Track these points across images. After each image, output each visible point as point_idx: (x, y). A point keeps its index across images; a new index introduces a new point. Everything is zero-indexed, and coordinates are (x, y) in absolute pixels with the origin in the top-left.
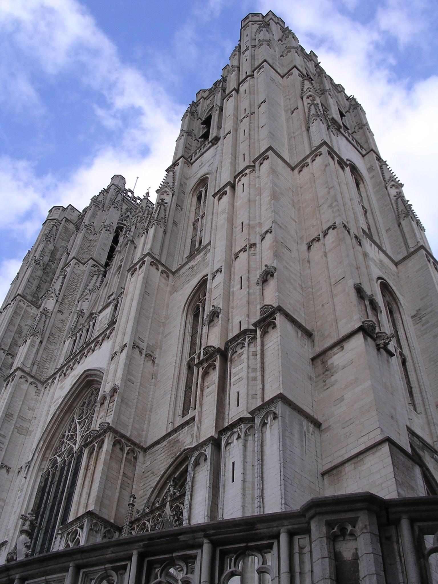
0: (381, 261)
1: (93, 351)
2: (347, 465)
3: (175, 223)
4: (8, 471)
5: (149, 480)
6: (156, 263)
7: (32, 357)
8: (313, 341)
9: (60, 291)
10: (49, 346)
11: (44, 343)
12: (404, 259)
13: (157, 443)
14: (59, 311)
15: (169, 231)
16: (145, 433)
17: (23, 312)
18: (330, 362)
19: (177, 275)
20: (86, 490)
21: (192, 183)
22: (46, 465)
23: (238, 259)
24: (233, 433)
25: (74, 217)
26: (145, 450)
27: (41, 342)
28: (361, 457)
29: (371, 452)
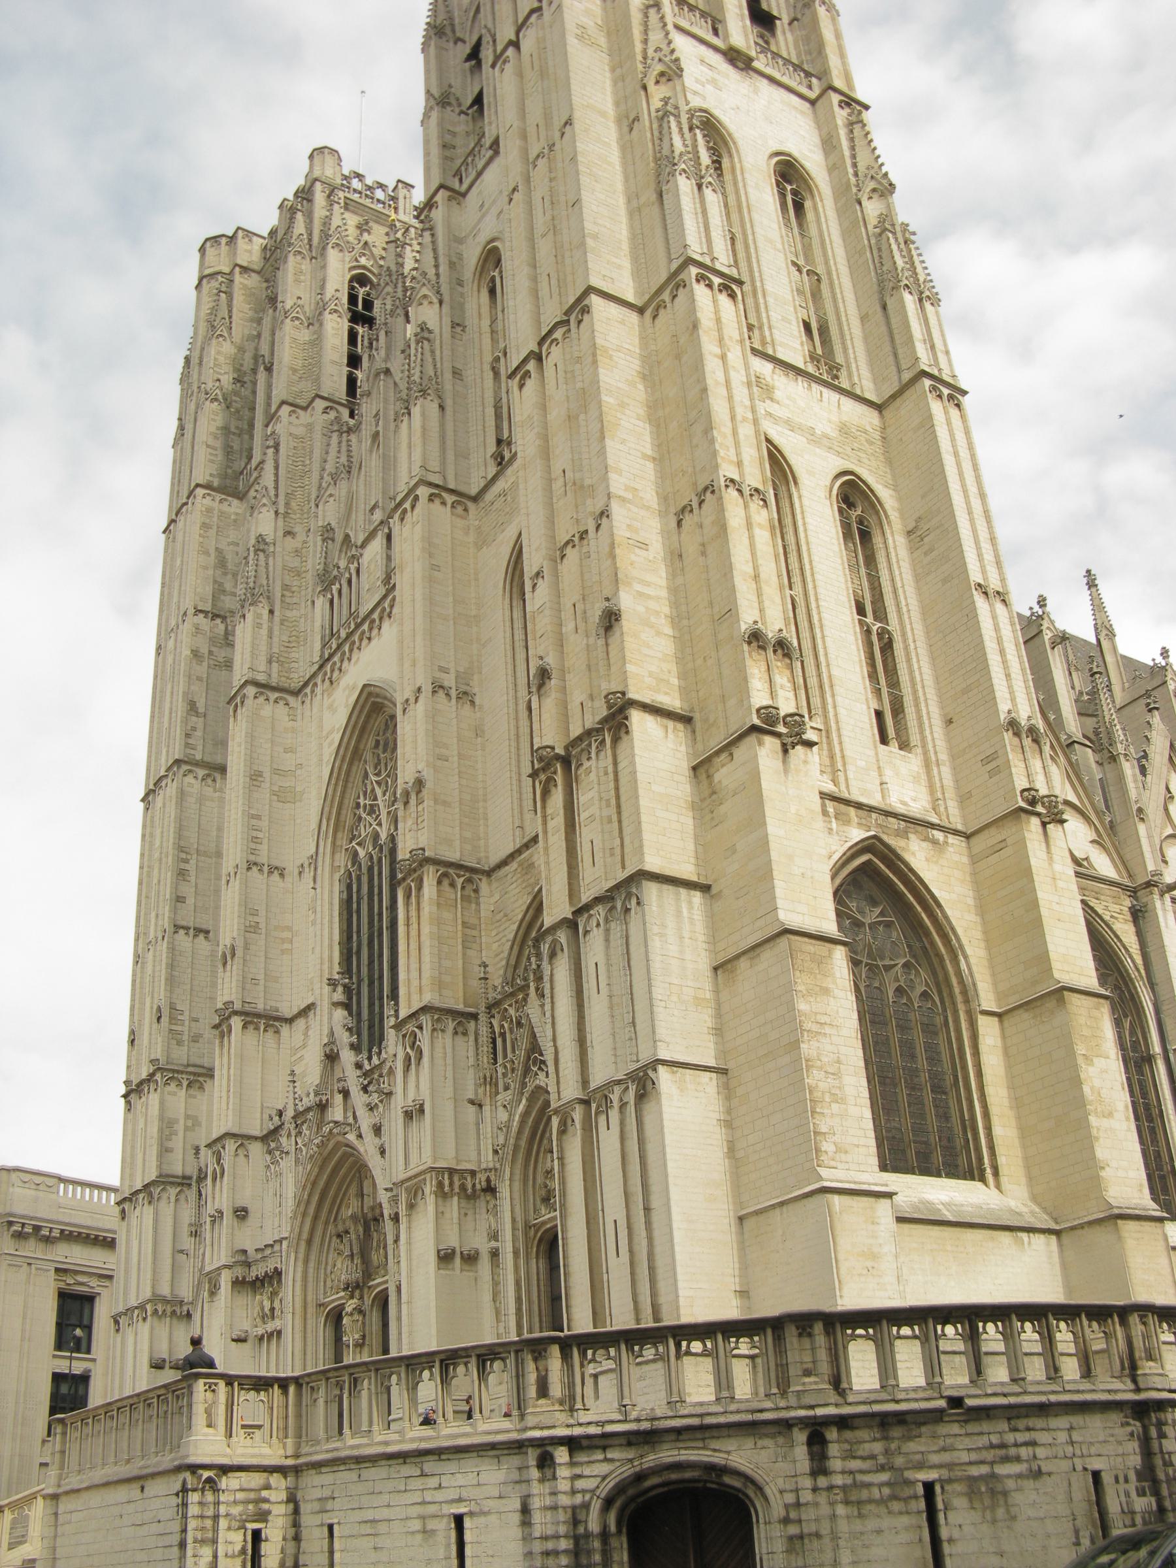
0: (844, 429)
1: (369, 639)
2: (742, 959)
3: (456, 373)
4: (282, 875)
5: (502, 927)
6: (439, 491)
7: (263, 648)
8: (694, 732)
9: (276, 488)
10: (288, 614)
11: (277, 613)
12: (894, 397)
13: (504, 863)
14: (288, 533)
15: (449, 403)
16: (482, 842)
17: (215, 519)
18: (717, 777)
19: (482, 505)
21: (472, 255)
22: (342, 860)
23: (565, 560)
24: (591, 916)
27: (271, 612)
28: (758, 951)
29: (768, 946)
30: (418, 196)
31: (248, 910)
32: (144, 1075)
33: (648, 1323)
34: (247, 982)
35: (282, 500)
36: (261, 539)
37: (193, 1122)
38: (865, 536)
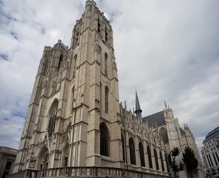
3: (70, 67)
6: (67, 79)
13: (67, 119)
15: (69, 70)
20: (57, 128)
21: (74, 55)
22: (50, 116)
25: (50, 50)
26: (66, 120)
27: (47, 89)
30: (69, 48)
31: (39, 120)
32: (24, 137)
33: (76, 166)
34: (37, 128)
35: (49, 77)
36: (46, 81)
37: (29, 143)
38: (107, 92)
